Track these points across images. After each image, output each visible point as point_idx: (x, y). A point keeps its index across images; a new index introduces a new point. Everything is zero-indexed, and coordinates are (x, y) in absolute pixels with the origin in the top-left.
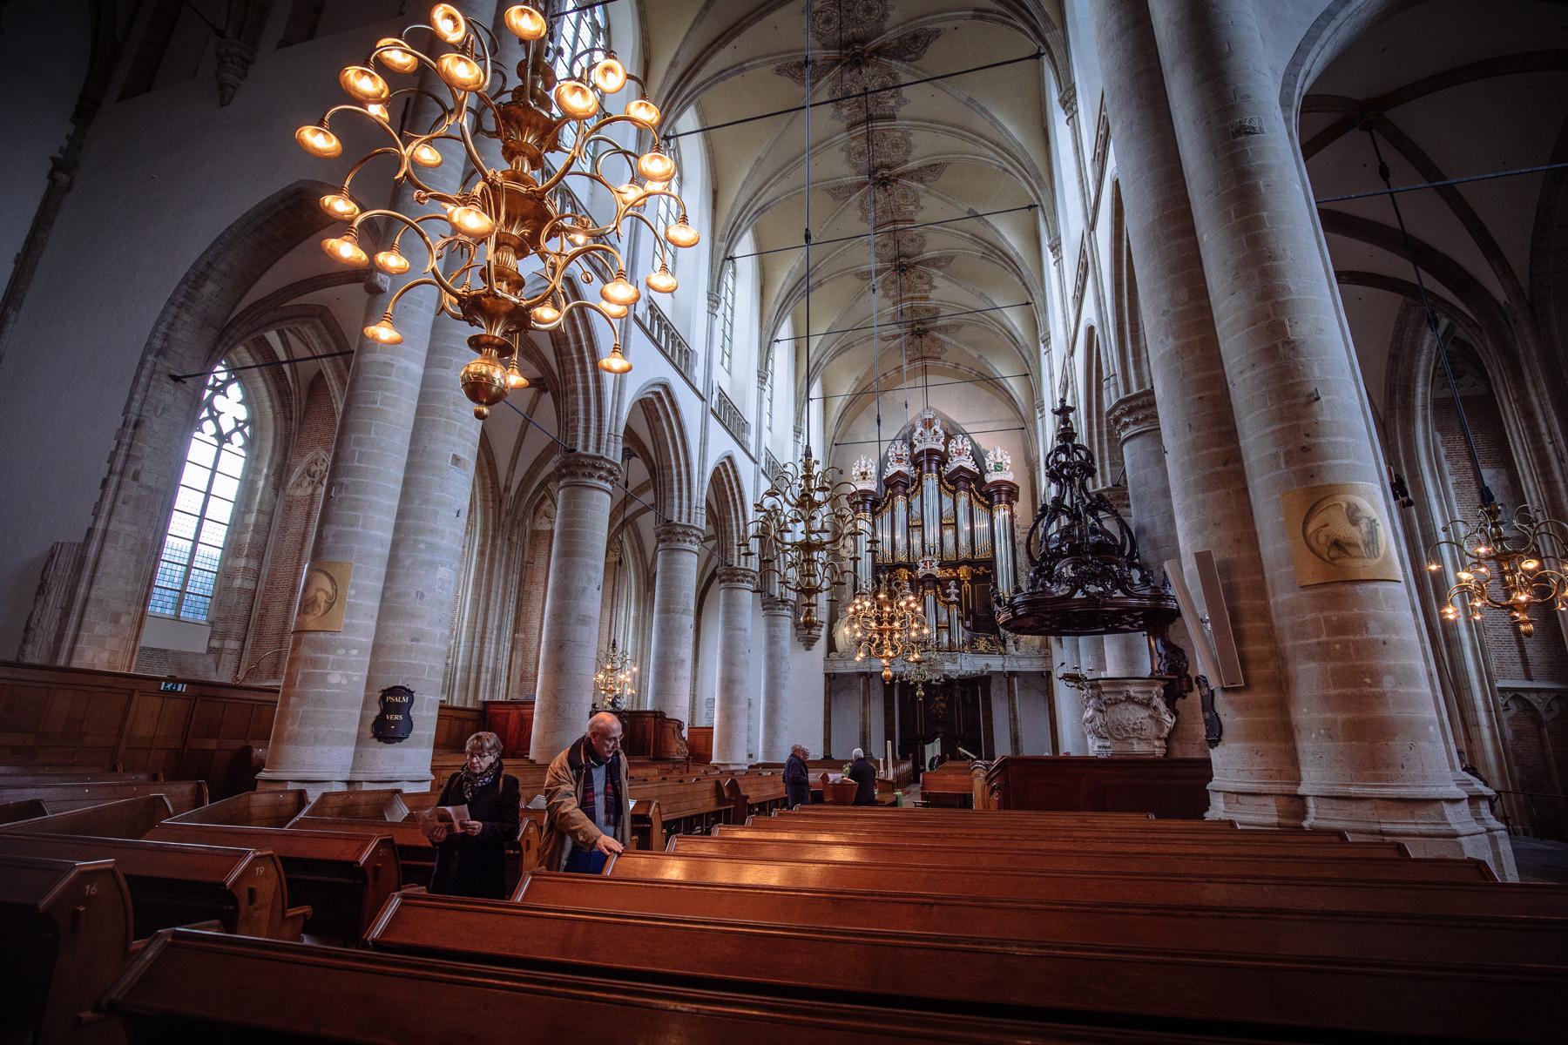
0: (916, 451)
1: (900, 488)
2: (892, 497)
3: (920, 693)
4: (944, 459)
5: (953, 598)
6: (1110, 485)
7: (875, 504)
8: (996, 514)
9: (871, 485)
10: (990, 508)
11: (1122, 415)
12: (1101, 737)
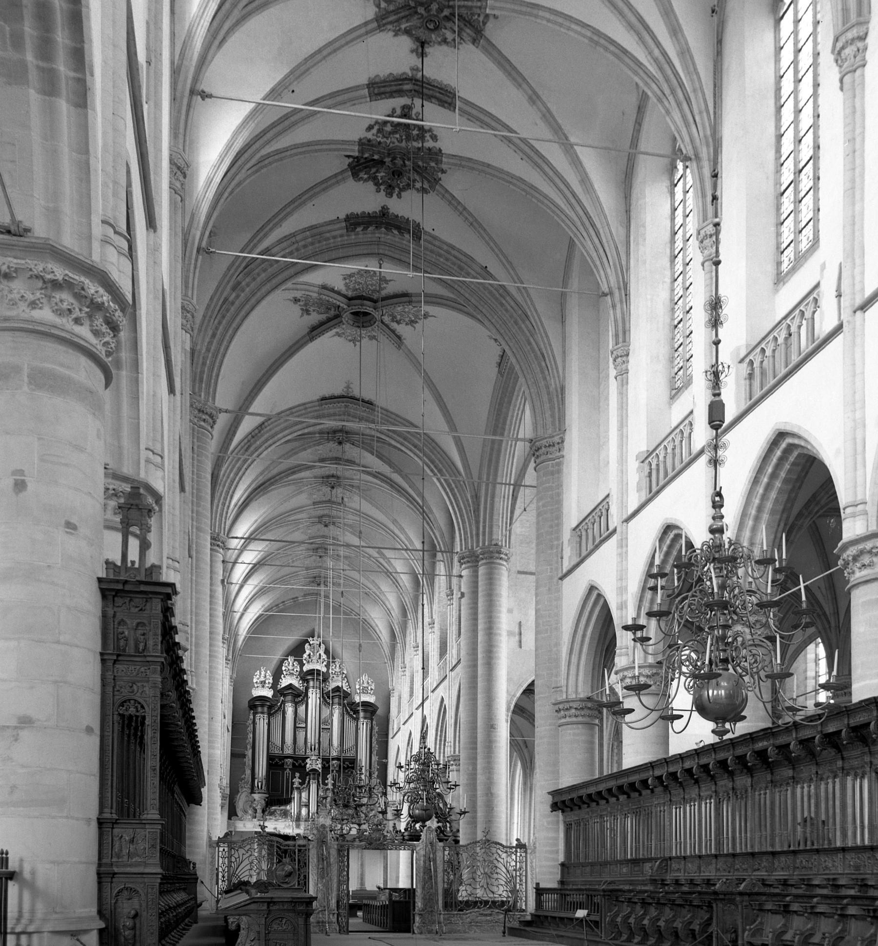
0: (305, 669)
1: (289, 698)
2: (283, 702)
4: (326, 678)
7: (270, 708)
9: (269, 693)
10: (357, 719)
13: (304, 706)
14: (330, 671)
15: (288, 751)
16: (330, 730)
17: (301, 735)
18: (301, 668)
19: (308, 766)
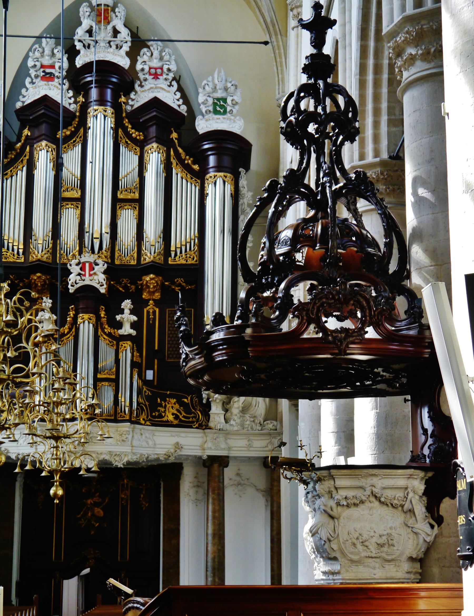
0: (79, 62)
3: (56, 490)
5: (127, 330)
6: (385, 156)
8: (209, 189)
10: (200, 176)
11: (407, 42)
12: (330, 558)
13: (78, 149)
14: (139, 66)
15: (39, 252)
16: (139, 203)
17: (70, 217)
18: (71, 60)
19: (72, 278)
